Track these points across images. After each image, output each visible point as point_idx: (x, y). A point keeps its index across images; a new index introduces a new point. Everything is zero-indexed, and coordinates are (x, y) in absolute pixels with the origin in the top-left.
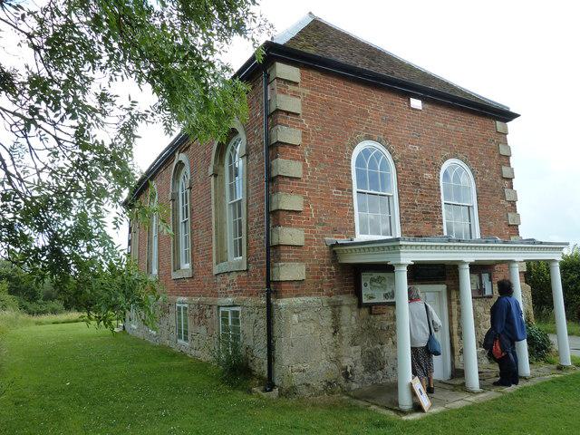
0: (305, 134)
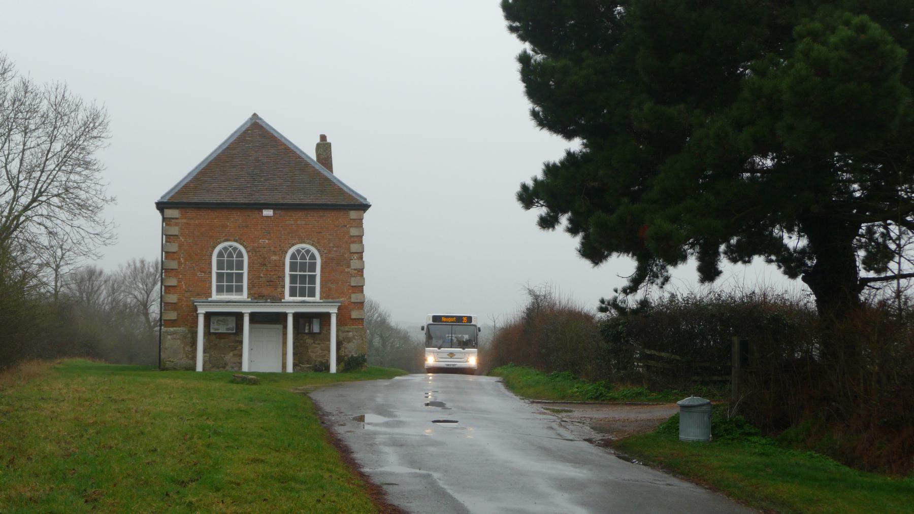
0: (180, 246)
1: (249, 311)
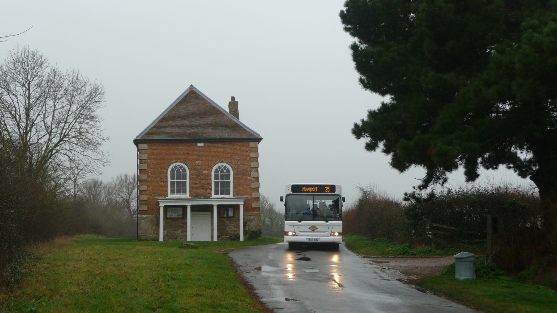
0: (149, 166)
1: (191, 204)
